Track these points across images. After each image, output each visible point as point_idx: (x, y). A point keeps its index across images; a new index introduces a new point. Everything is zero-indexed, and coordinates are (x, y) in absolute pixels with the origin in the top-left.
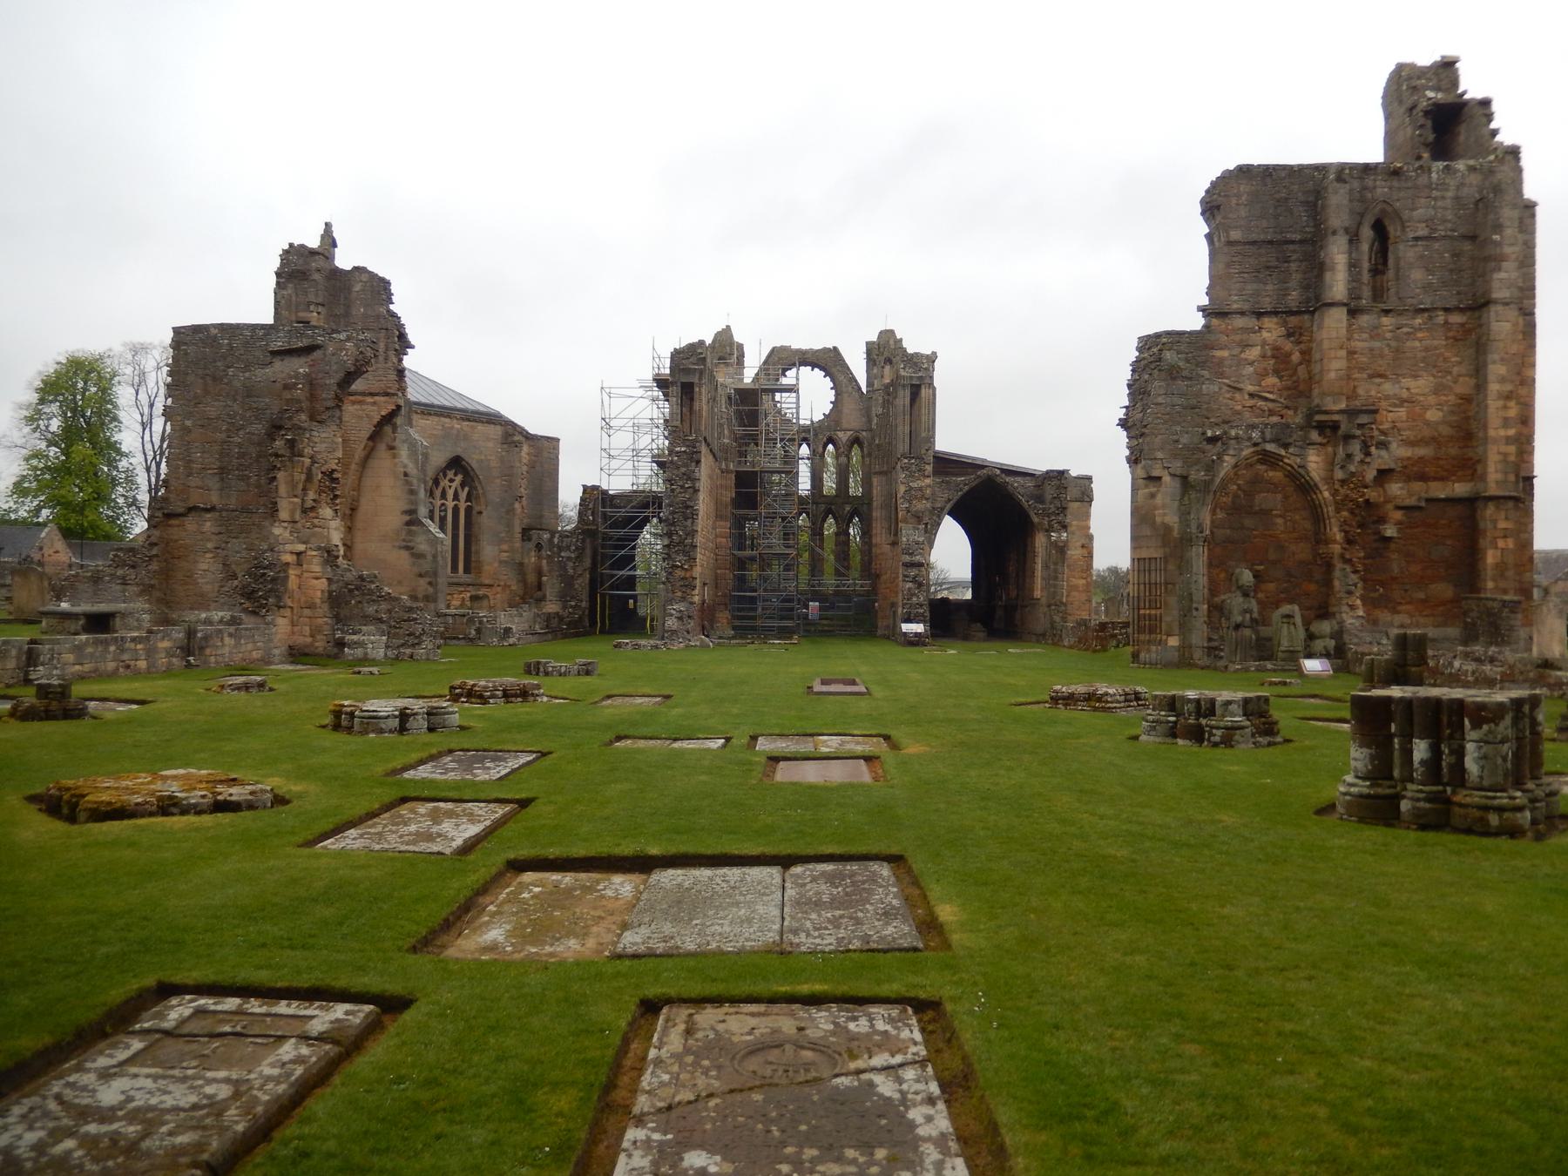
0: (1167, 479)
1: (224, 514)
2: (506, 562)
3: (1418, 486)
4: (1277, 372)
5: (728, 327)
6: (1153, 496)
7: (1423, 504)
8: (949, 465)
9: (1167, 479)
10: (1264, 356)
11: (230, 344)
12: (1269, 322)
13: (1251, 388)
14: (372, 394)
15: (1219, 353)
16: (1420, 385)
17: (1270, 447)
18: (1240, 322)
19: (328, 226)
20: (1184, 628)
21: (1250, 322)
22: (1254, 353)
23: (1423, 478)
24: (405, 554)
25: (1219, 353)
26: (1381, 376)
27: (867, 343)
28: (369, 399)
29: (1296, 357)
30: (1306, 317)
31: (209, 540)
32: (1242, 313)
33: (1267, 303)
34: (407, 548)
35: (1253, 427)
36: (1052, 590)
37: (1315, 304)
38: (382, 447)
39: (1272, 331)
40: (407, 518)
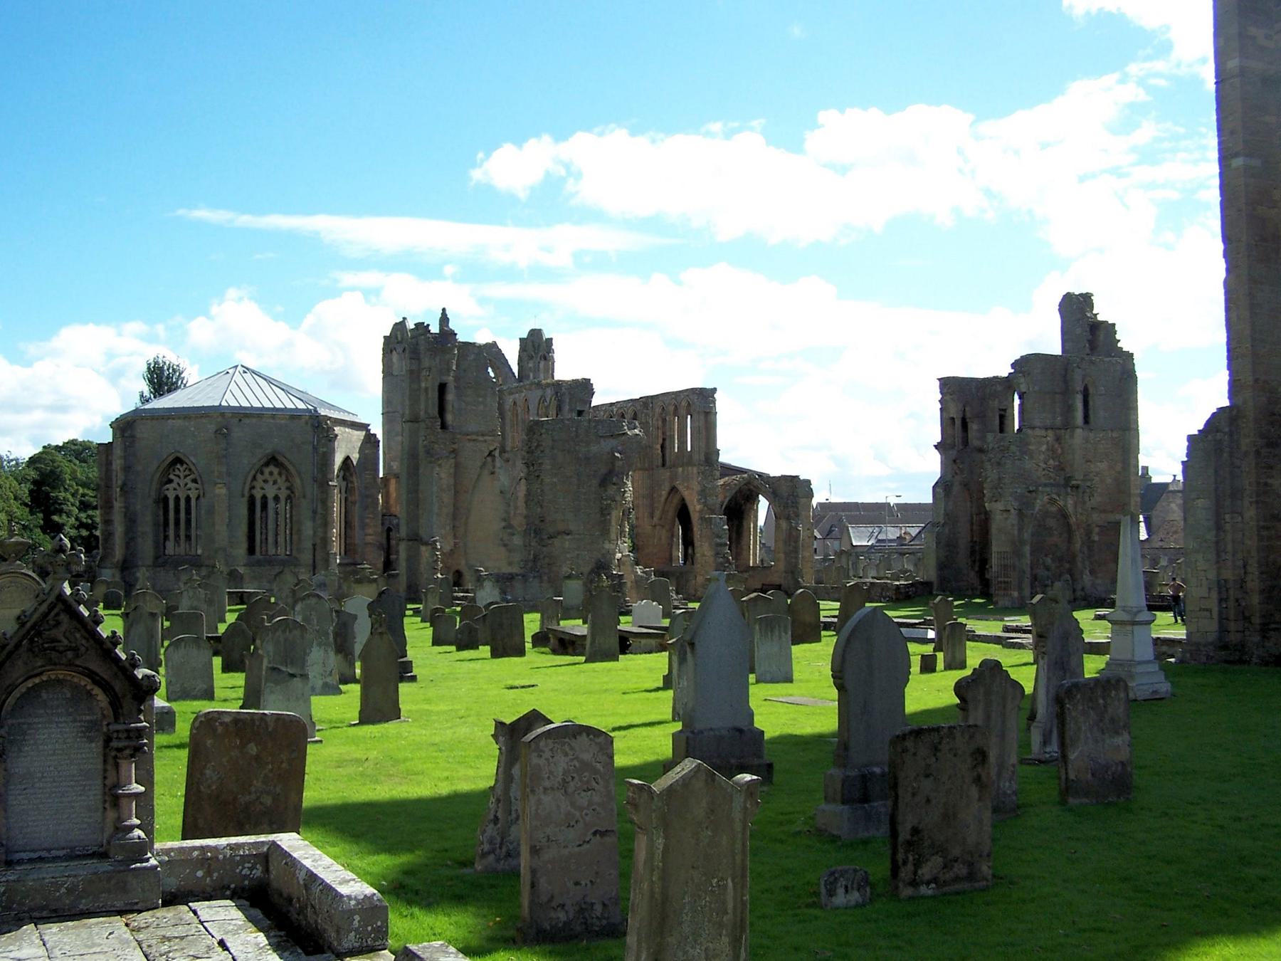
0: (1012, 511)
1: (577, 536)
2: (370, 543)
3: (1103, 516)
4: (1053, 459)
5: (404, 319)
6: (1006, 519)
7: (1106, 524)
8: (729, 470)
9: (1012, 511)
10: (1048, 450)
11: (576, 431)
12: (1050, 433)
13: (1044, 466)
14: (483, 435)
15: (1031, 447)
16: (1103, 466)
17: (1054, 496)
18: (1039, 432)
19: (444, 310)
20: (1020, 589)
21: (1043, 433)
22: (1044, 448)
23: (1104, 511)
24: (503, 549)
25: (1031, 447)
26: (1090, 461)
27: (521, 340)
28: (481, 438)
29: (1059, 451)
30: (1063, 431)
31: (569, 553)
32: (1040, 428)
33: (1048, 422)
34: (505, 545)
35: (1045, 485)
36: (793, 560)
37: (1068, 425)
38: (486, 472)
39: (1051, 436)
40: (503, 524)
